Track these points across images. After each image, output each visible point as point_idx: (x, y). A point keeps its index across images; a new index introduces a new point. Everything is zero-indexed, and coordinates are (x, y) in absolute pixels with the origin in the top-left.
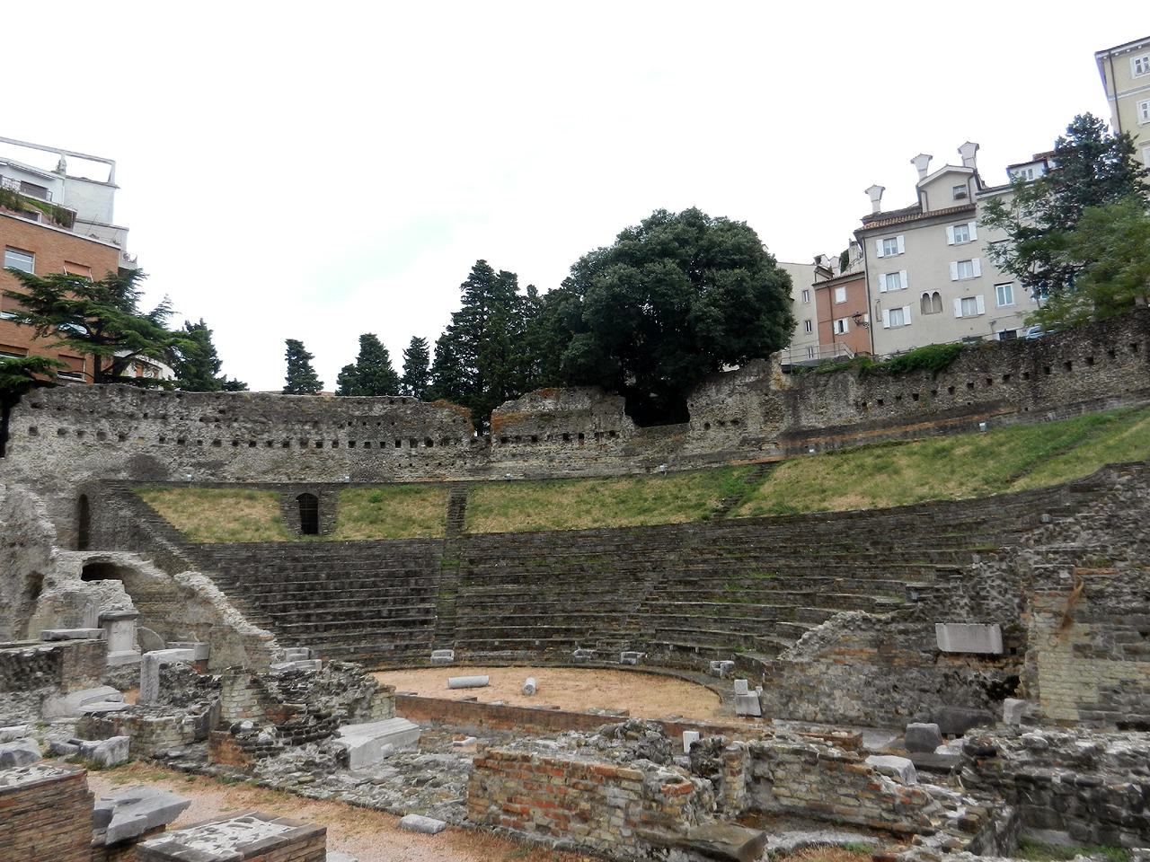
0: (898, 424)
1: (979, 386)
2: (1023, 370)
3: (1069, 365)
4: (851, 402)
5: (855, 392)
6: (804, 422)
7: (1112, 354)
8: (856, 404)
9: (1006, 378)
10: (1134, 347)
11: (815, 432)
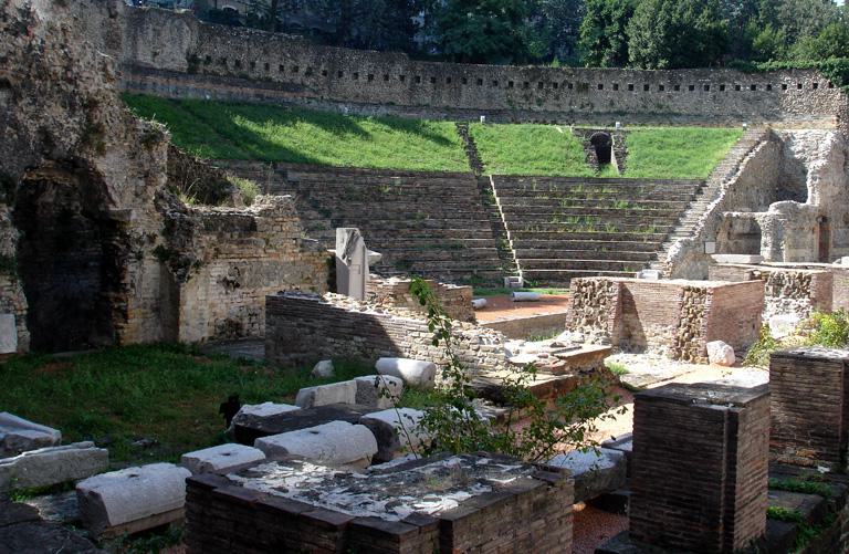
0: (227, 84)
1: (288, 70)
2: (322, 68)
3: (356, 75)
4: (184, 51)
5: (189, 40)
6: (140, 58)
7: (386, 78)
8: (188, 54)
9: (310, 69)
10: (402, 78)
11: (151, 71)
